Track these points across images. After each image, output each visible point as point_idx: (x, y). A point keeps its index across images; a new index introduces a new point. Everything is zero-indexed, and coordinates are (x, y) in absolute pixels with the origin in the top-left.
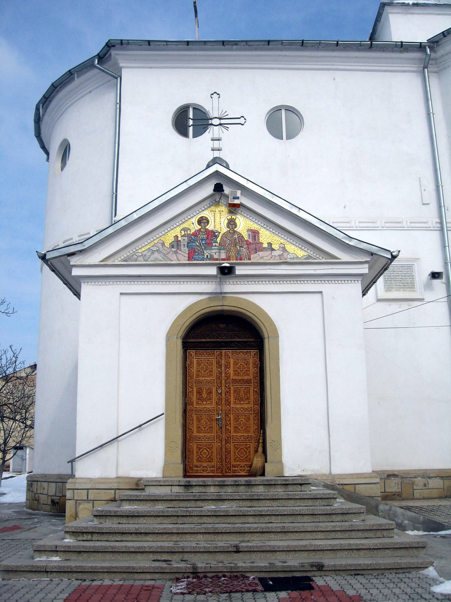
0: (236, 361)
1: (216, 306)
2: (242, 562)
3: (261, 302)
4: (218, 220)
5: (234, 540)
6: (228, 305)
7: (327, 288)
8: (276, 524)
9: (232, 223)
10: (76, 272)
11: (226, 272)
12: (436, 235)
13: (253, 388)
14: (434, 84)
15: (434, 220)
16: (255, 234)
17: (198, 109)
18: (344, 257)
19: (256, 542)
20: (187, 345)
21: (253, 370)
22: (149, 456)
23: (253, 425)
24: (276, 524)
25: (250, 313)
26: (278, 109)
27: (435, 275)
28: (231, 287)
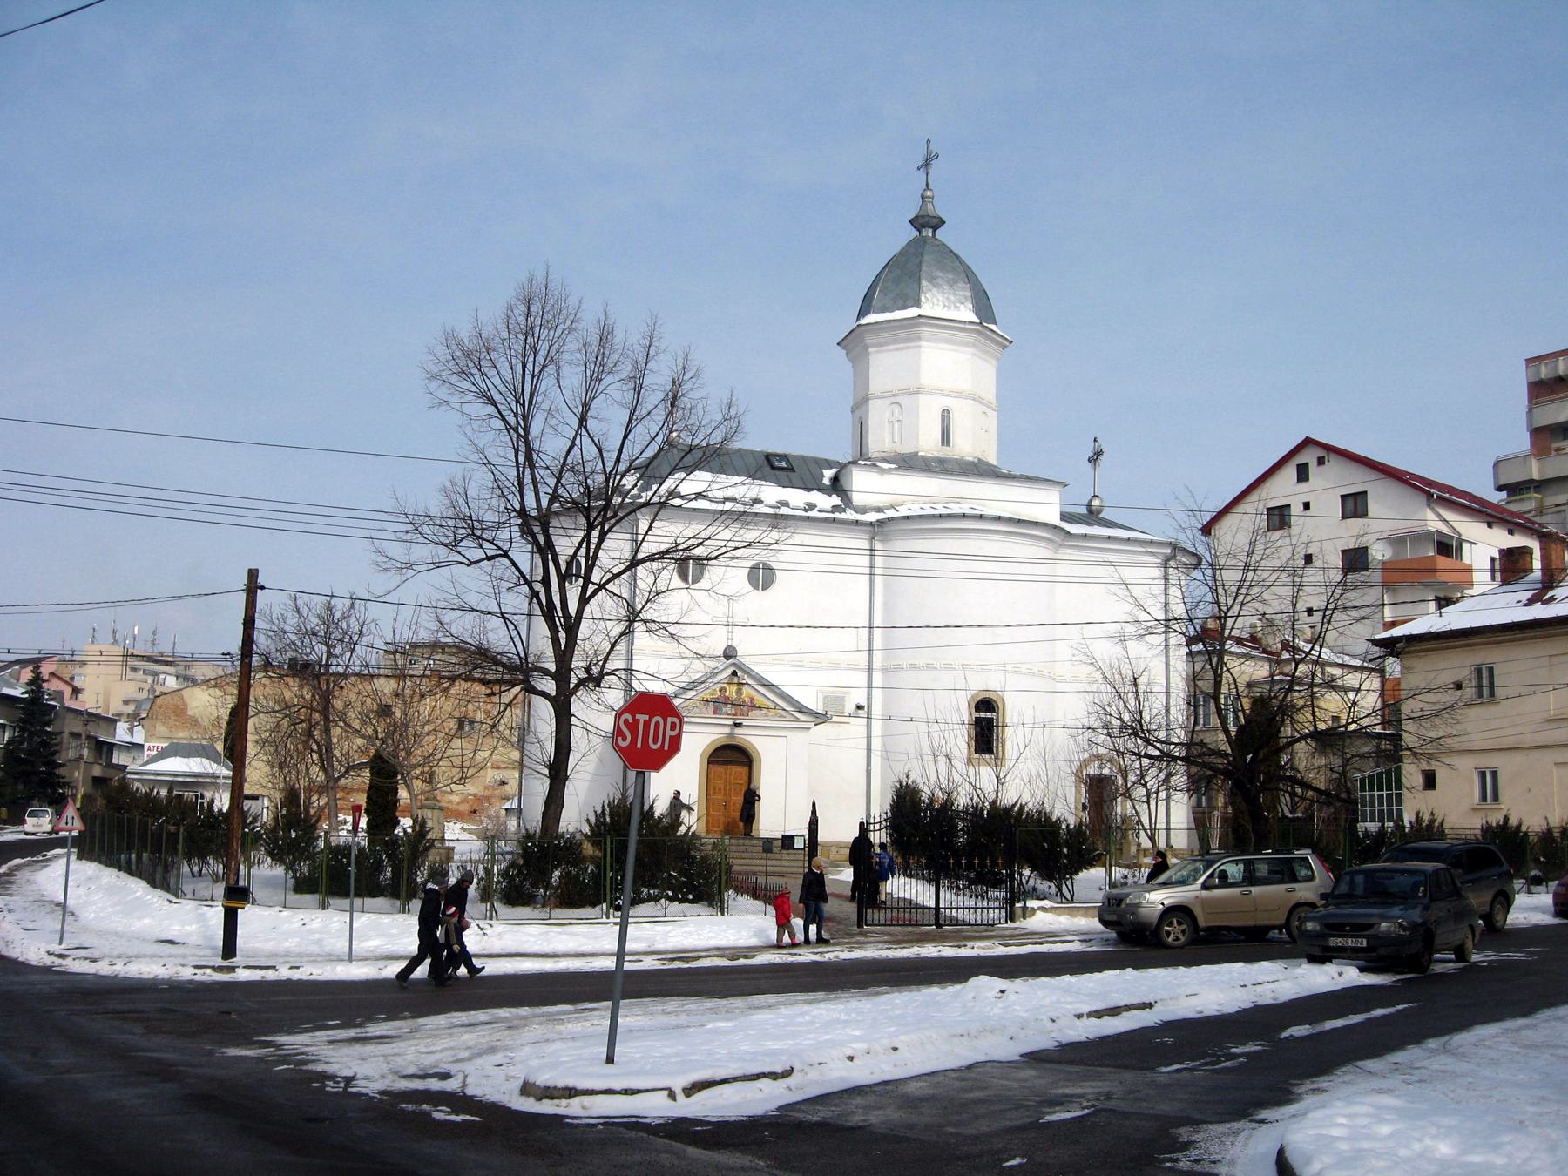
0: (738, 771)
4: (731, 691)
9: (739, 692)
11: (737, 725)
12: (866, 674)
15: (864, 663)
16: (752, 699)
21: (745, 778)
25: (746, 746)
27: (859, 707)
28: (738, 731)
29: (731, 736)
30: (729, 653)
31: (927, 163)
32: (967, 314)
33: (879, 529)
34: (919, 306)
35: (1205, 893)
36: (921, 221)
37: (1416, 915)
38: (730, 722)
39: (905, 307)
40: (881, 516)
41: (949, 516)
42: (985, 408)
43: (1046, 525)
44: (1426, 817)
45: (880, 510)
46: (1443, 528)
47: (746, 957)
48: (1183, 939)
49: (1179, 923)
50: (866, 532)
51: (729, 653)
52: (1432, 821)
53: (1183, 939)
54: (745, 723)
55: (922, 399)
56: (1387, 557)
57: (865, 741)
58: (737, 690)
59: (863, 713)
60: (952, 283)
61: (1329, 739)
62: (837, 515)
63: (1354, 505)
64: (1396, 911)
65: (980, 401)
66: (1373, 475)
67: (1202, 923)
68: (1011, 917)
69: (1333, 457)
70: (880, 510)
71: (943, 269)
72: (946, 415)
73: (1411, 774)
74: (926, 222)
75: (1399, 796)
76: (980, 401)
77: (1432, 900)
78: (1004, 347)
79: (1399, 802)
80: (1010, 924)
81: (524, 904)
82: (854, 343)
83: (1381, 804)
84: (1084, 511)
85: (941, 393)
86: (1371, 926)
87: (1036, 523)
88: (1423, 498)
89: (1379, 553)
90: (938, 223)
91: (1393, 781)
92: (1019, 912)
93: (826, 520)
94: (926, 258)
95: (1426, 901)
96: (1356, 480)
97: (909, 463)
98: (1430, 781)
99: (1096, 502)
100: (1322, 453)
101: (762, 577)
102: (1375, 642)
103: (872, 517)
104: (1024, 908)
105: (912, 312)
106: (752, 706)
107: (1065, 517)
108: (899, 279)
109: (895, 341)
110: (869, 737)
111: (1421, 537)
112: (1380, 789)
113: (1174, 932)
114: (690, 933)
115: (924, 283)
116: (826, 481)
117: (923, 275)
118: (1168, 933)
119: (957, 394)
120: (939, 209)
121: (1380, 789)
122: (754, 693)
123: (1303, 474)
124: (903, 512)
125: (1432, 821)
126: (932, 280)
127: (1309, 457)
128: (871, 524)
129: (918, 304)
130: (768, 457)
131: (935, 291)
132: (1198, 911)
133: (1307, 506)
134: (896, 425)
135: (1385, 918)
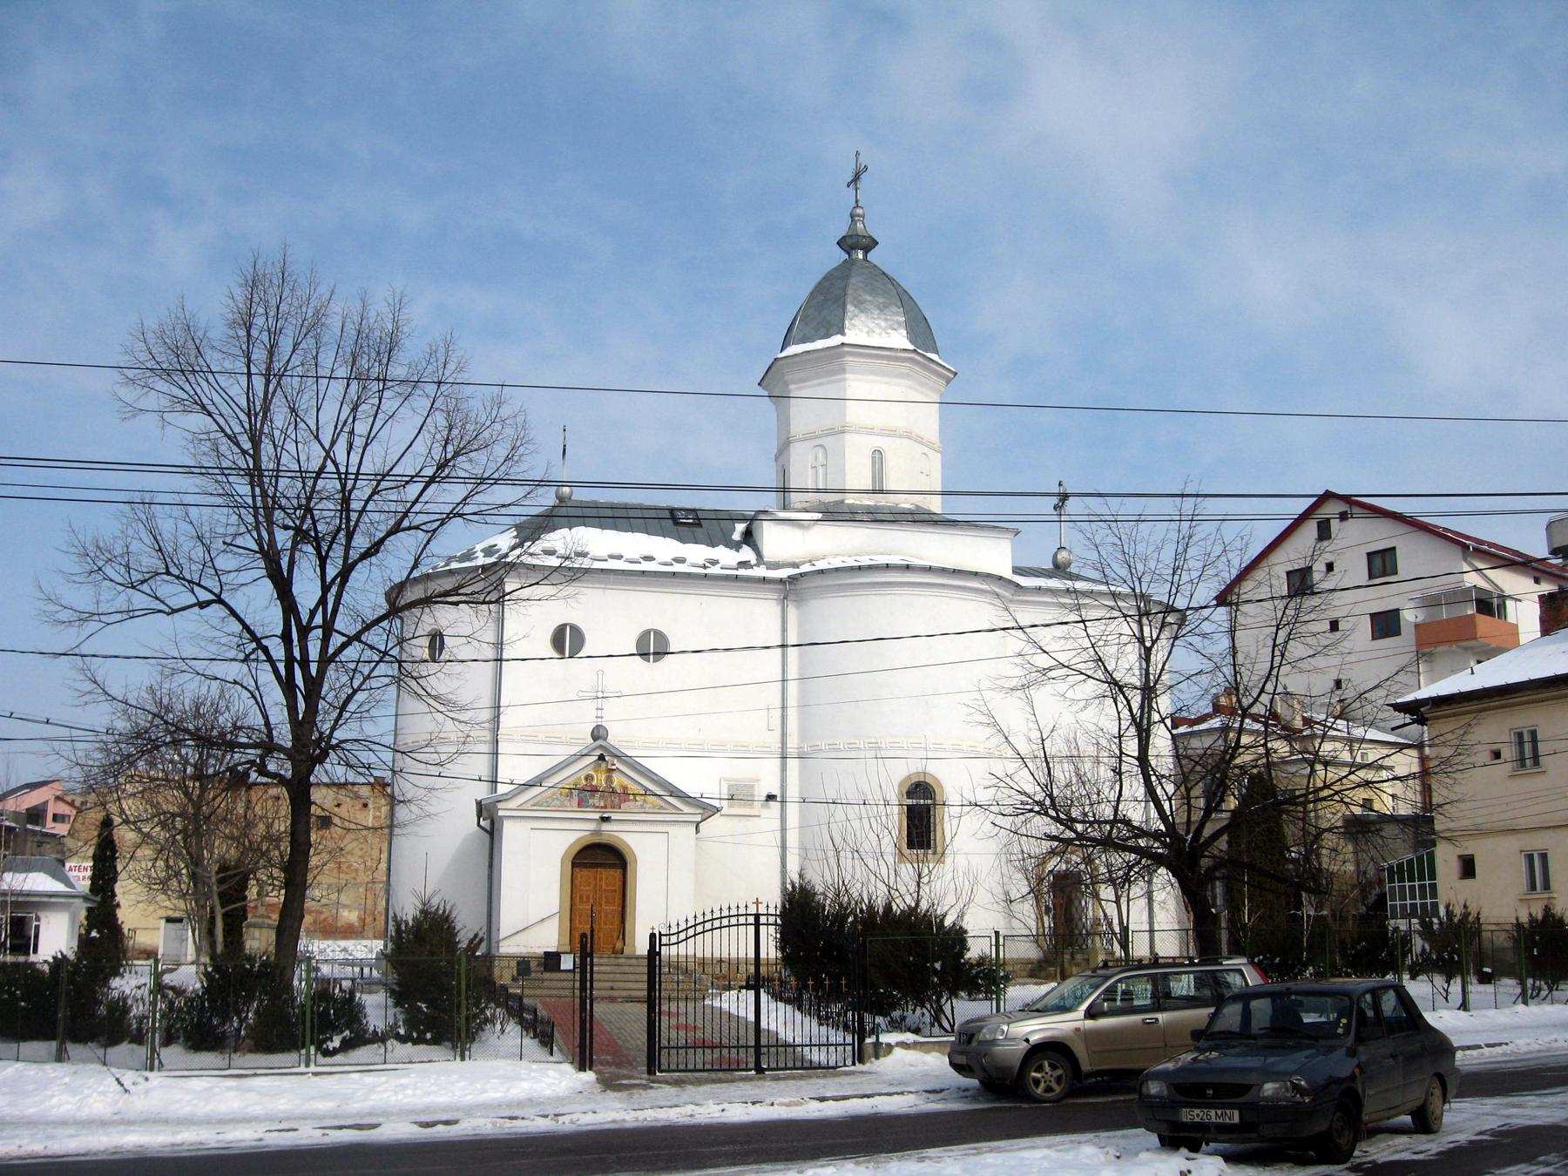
0: (609, 876)
1: (596, 840)
2: (615, 993)
3: (624, 836)
4: (600, 780)
5: (608, 985)
6: (604, 840)
7: (672, 829)
8: (632, 977)
9: (609, 780)
10: (501, 813)
11: (605, 820)
13: (618, 896)
14: (792, 611)
16: (625, 788)
17: (576, 631)
18: (686, 809)
19: (621, 985)
20: (574, 865)
22: (548, 938)
23: (617, 922)
24: (632, 977)
26: (647, 632)
27: (771, 797)
28: (606, 827)
29: (597, 832)
30: (598, 734)
31: (857, 178)
32: (899, 339)
33: (794, 587)
34: (843, 334)
35: (1089, 1023)
36: (850, 241)
37: (1339, 1065)
38: (597, 816)
39: (827, 336)
40: (797, 571)
41: (870, 568)
42: (926, 450)
43: (988, 577)
44: (1458, 911)
45: (796, 565)
46: (1482, 584)
47: (447, 1123)
48: (1058, 1089)
49: (1053, 1067)
50: (774, 591)
51: (598, 734)
52: (1466, 915)
53: (1058, 1089)
54: (614, 816)
55: (847, 436)
56: (1420, 619)
57: (778, 834)
58: (605, 779)
59: (775, 806)
60: (882, 309)
61: (1362, 828)
62: (742, 572)
63: (1382, 564)
64: (1300, 1056)
65: (919, 440)
66: (1401, 528)
67: (1086, 1066)
68: (860, 1057)
69: (1356, 510)
70: (796, 565)
71: (873, 292)
72: (878, 457)
73: (1446, 859)
74: (855, 242)
75: (1434, 887)
76: (919, 440)
77: (1360, 1040)
78: (948, 381)
79: (1434, 894)
80: (859, 1067)
81: (211, 1049)
82: (775, 382)
83: (1413, 897)
84: (1050, 566)
85: (869, 431)
86: (1246, 1088)
87: (976, 574)
88: (1458, 551)
89: (1409, 616)
90: (870, 244)
91: (1425, 869)
92: (869, 1050)
93: (727, 578)
94: (853, 280)
95: (1350, 1040)
96: (1380, 536)
97: (835, 513)
98: (1468, 868)
99: (1063, 556)
100: (1342, 507)
101: (653, 647)
102: (1398, 707)
103: (783, 573)
104: (877, 1044)
105: (836, 340)
106: (625, 794)
107: (1017, 570)
108: (824, 308)
109: (818, 376)
110: (783, 830)
111: (1459, 596)
112: (1411, 879)
113: (1045, 1077)
114: (404, 1087)
115: (850, 307)
116: (737, 536)
117: (849, 299)
118: (1037, 1082)
119: (891, 433)
120: (871, 226)
121: (1411, 879)
122: (626, 782)
123: (1324, 532)
124: (821, 565)
125: (1466, 915)
126: (859, 304)
127: (1331, 509)
128: (781, 581)
129: (843, 334)
130: (672, 511)
131: (863, 317)
132: (1080, 1050)
133: (1330, 567)
134: (821, 470)
135: (1271, 1075)
